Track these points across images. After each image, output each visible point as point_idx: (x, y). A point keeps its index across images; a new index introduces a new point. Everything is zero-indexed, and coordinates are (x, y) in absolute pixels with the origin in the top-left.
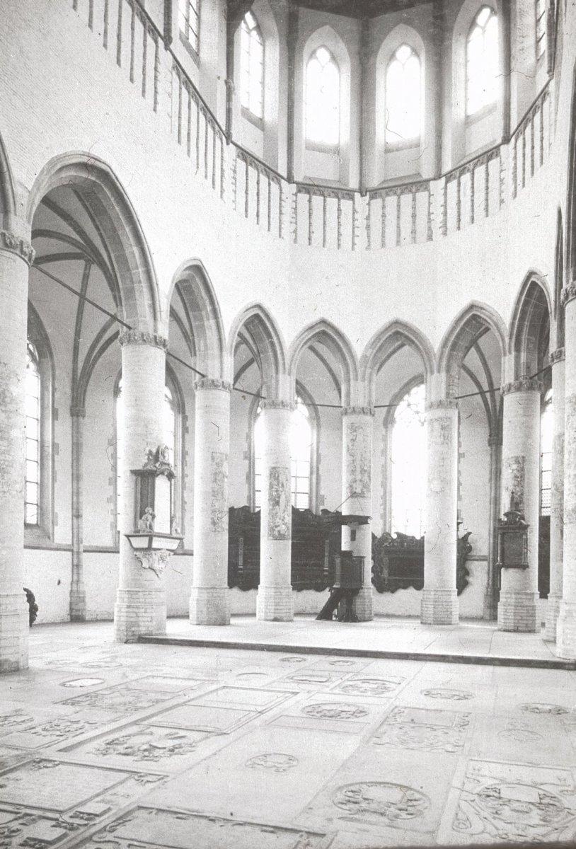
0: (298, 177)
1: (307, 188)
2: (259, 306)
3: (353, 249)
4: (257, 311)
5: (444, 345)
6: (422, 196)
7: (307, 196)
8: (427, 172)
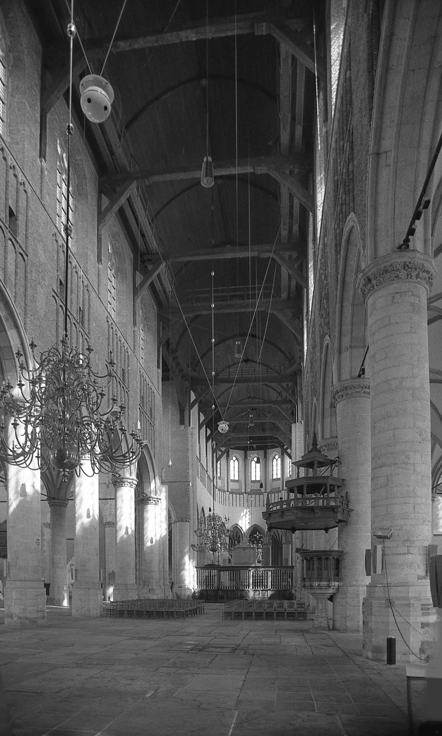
0: (230, 490)
6: (261, 496)
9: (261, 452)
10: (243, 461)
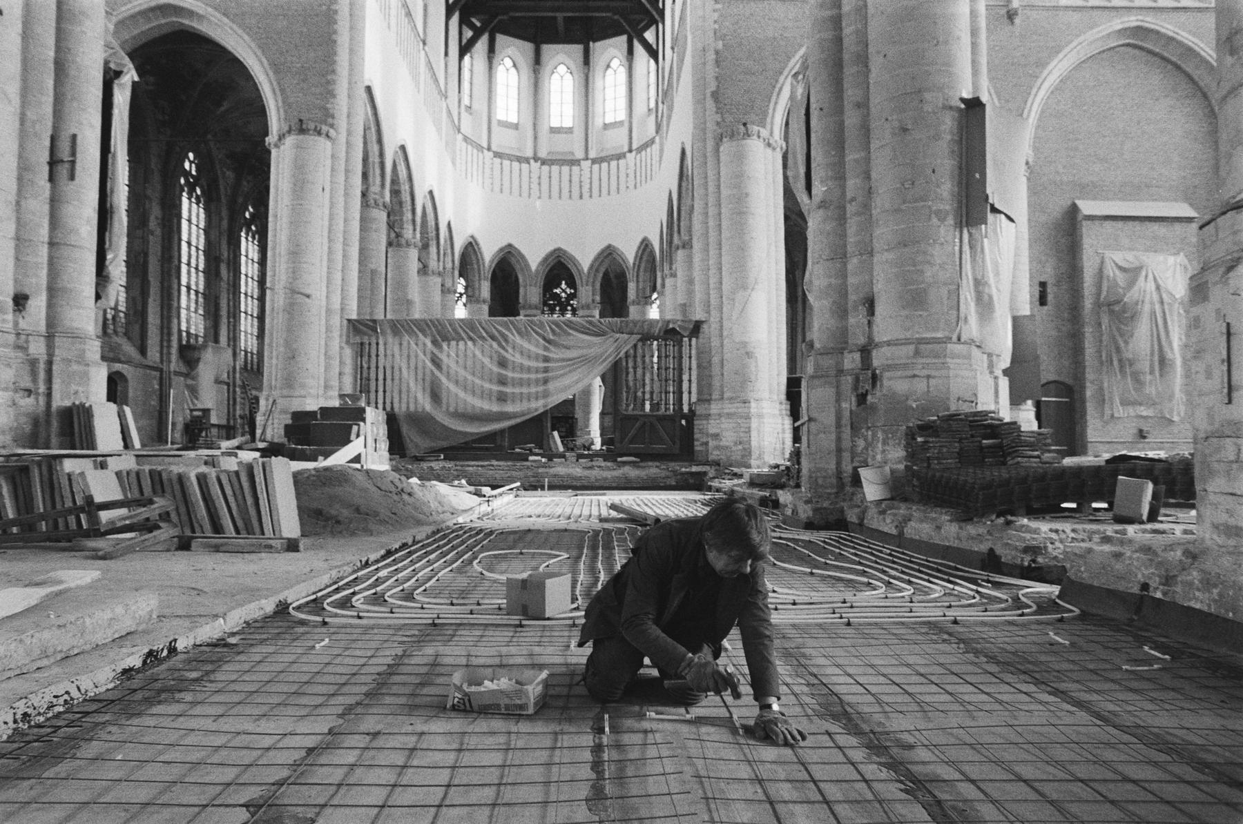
0: (494, 148)
1: (498, 155)
2: (472, 237)
3: (529, 197)
4: (471, 240)
6: (575, 169)
8: (579, 154)
9: (577, 49)
10: (532, 75)
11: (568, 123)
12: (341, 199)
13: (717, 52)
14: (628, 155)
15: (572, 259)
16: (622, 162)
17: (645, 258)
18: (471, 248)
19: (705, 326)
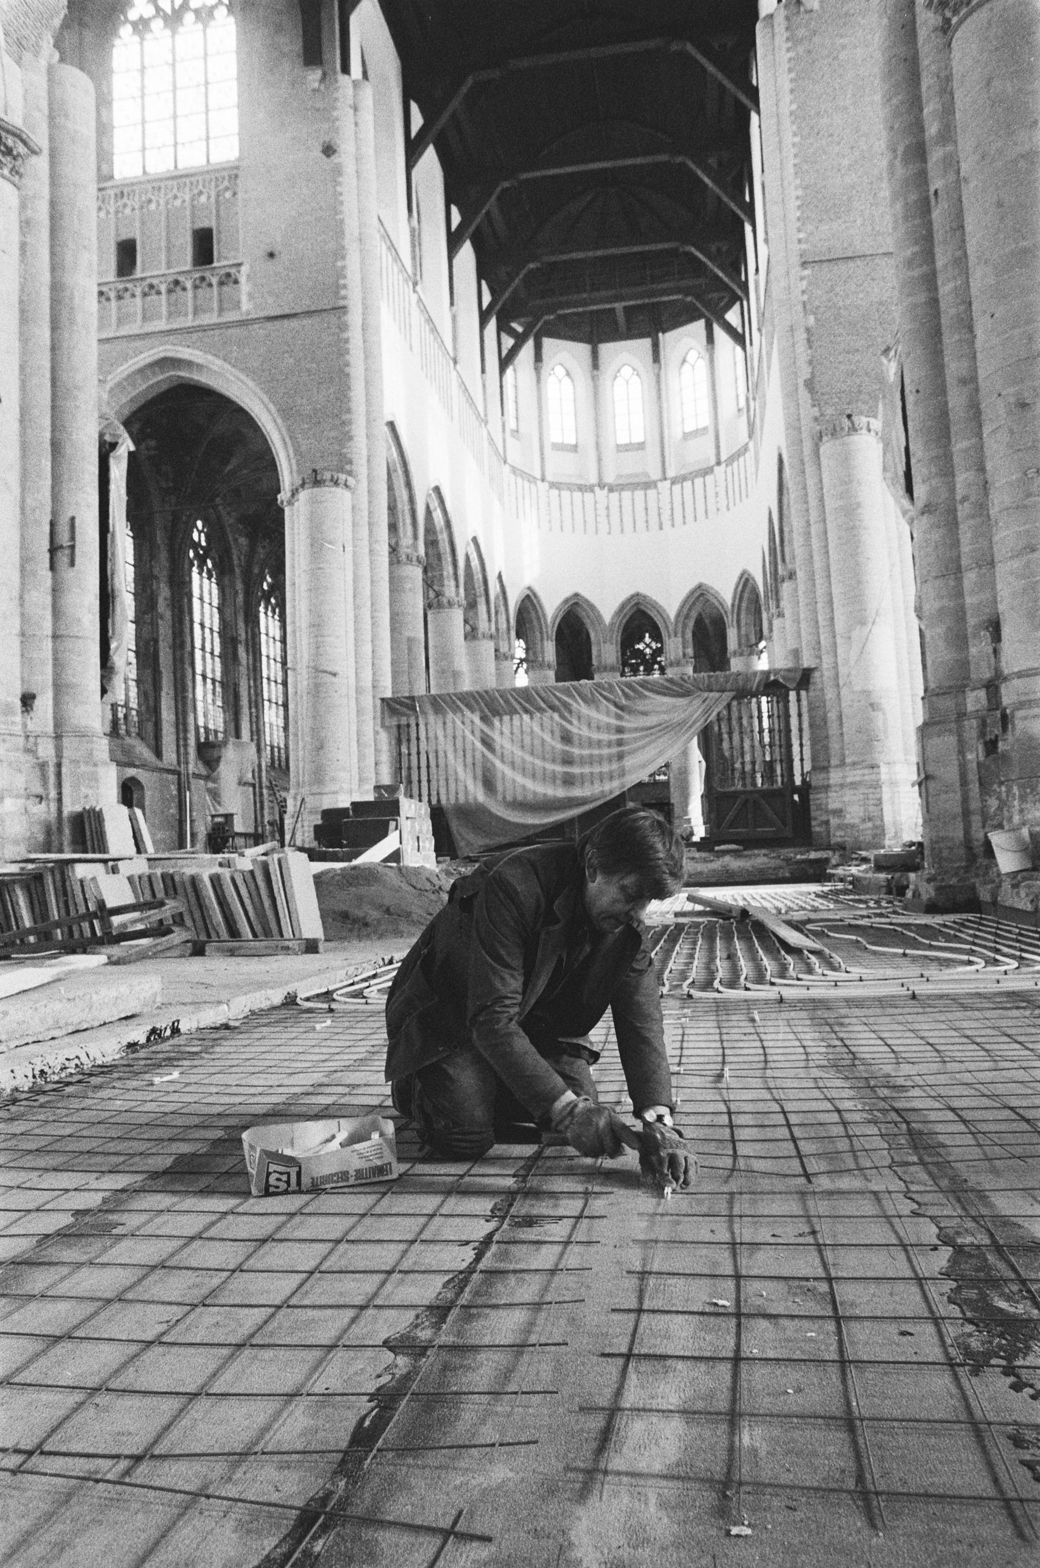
0: (549, 477)
2: (529, 588)
5: (678, 616)
6: (652, 493)
7: (556, 492)
8: (655, 474)
9: (646, 343)
10: (590, 381)
11: (638, 438)
12: (367, 560)
13: (808, 330)
14: (716, 468)
15: (655, 605)
16: (709, 478)
17: (746, 595)
18: (529, 605)
19: (817, 674)
